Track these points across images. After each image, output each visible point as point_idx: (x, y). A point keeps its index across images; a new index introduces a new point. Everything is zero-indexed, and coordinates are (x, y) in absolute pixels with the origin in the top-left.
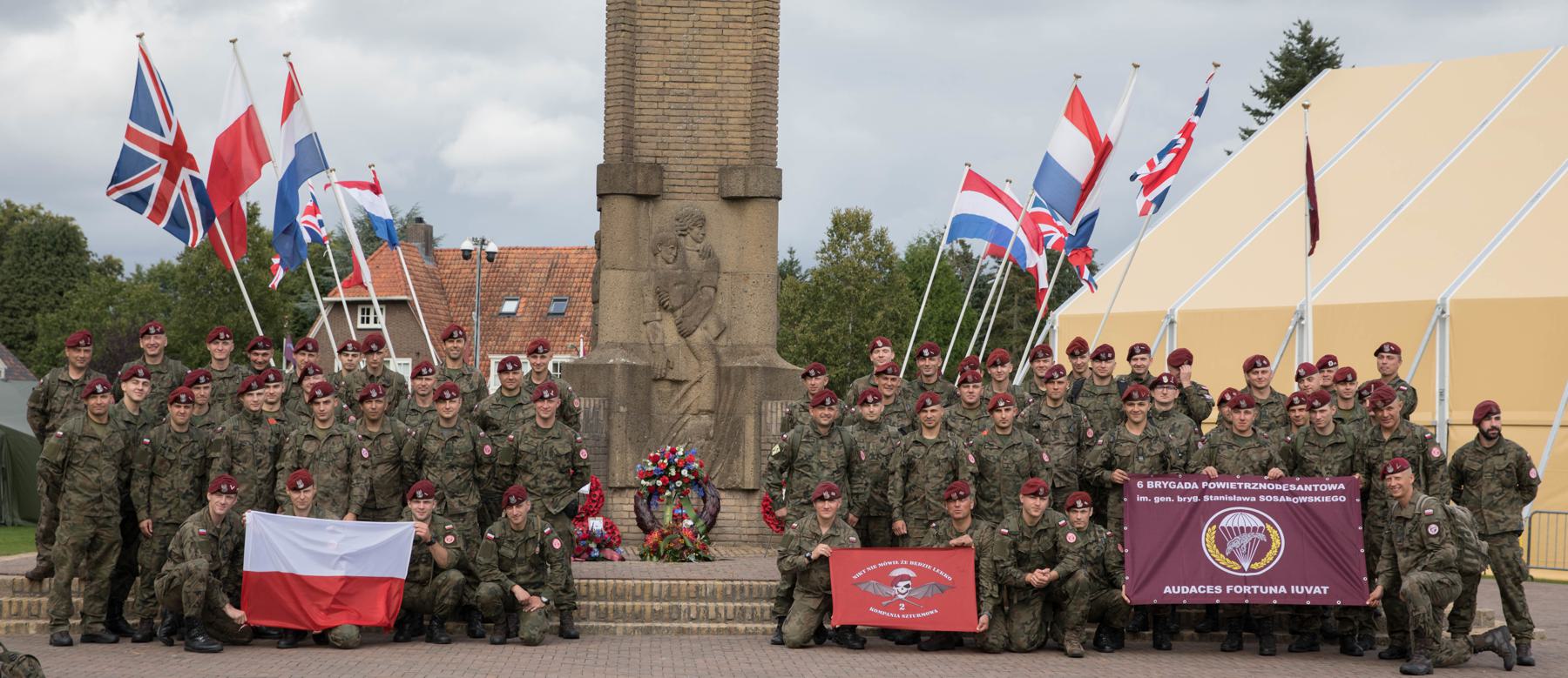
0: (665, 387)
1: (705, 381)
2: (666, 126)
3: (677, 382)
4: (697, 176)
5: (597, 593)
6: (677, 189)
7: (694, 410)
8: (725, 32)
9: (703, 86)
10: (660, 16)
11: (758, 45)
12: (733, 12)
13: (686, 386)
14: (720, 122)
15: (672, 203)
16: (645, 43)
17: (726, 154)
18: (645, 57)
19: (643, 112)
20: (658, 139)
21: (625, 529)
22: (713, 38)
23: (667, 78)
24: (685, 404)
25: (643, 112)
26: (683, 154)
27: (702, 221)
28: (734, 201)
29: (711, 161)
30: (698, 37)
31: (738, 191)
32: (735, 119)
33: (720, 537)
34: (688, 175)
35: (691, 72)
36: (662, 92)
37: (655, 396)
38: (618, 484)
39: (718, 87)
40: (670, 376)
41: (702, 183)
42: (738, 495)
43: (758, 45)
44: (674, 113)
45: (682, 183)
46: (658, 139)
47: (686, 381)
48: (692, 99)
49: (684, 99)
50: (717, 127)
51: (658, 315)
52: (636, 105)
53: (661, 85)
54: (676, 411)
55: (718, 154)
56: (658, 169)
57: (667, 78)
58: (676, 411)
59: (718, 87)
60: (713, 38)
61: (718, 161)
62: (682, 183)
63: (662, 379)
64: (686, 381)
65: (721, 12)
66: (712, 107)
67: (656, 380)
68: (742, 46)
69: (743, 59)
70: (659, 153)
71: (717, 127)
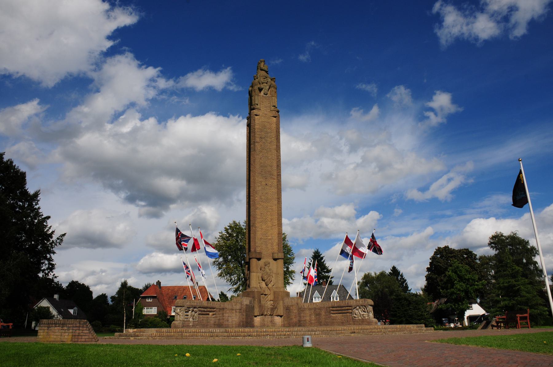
0: (263, 296)
1: (271, 294)
2: (262, 245)
3: (265, 295)
4: (268, 255)
5: (274, 331)
6: (264, 257)
7: (269, 300)
8: (273, 228)
9: (269, 237)
10: (260, 224)
11: (279, 230)
12: (274, 224)
13: (267, 295)
14: (272, 244)
15: (263, 260)
16: (258, 230)
17: (273, 251)
18: (258, 232)
19: (258, 242)
20: (261, 247)
21: (257, 324)
22: (270, 229)
23: (262, 236)
24: (267, 299)
25: (258, 242)
26: (265, 250)
27: (269, 263)
28: (275, 260)
29: (270, 252)
30: (267, 229)
31: (276, 257)
32: (275, 244)
33: (276, 325)
34: (266, 254)
35: (266, 235)
36: (261, 239)
37: (261, 297)
38: (256, 315)
39: (271, 238)
40: (264, 294)
41: (269, 256)
42: (279, 317)
43: (279, 230)
44: (263, 243)
45: (265, 256)
46: (261, 247)
47: (267, 295)
48: (266, 240)
49: (265, 240)
50: (272, 245)
51: (262, 281)
52: (256, 241)
53: (261, 237)
54: (265, 300)
55: (272, 250)
56: (260, 253)
57: (262, 236)
58: (265, 300)
59: (271, 238)
60: (270, 229)
61: (272, 252)
62: (265, 256)
63: (263, 294)
64: (267, 295)
65: (272, 224)
66: (270, 241)
67: (262, 294)
68: (276, 230)
69: (276, 233)
70: (261, 250)
71: (272, 245)
